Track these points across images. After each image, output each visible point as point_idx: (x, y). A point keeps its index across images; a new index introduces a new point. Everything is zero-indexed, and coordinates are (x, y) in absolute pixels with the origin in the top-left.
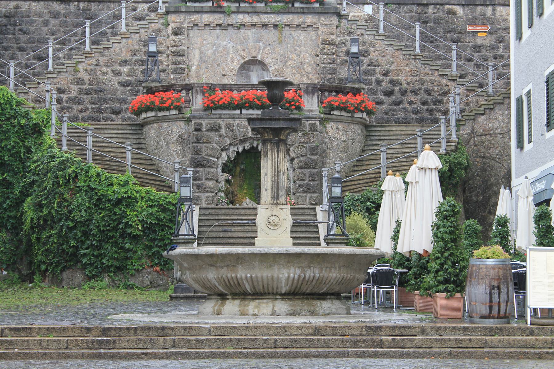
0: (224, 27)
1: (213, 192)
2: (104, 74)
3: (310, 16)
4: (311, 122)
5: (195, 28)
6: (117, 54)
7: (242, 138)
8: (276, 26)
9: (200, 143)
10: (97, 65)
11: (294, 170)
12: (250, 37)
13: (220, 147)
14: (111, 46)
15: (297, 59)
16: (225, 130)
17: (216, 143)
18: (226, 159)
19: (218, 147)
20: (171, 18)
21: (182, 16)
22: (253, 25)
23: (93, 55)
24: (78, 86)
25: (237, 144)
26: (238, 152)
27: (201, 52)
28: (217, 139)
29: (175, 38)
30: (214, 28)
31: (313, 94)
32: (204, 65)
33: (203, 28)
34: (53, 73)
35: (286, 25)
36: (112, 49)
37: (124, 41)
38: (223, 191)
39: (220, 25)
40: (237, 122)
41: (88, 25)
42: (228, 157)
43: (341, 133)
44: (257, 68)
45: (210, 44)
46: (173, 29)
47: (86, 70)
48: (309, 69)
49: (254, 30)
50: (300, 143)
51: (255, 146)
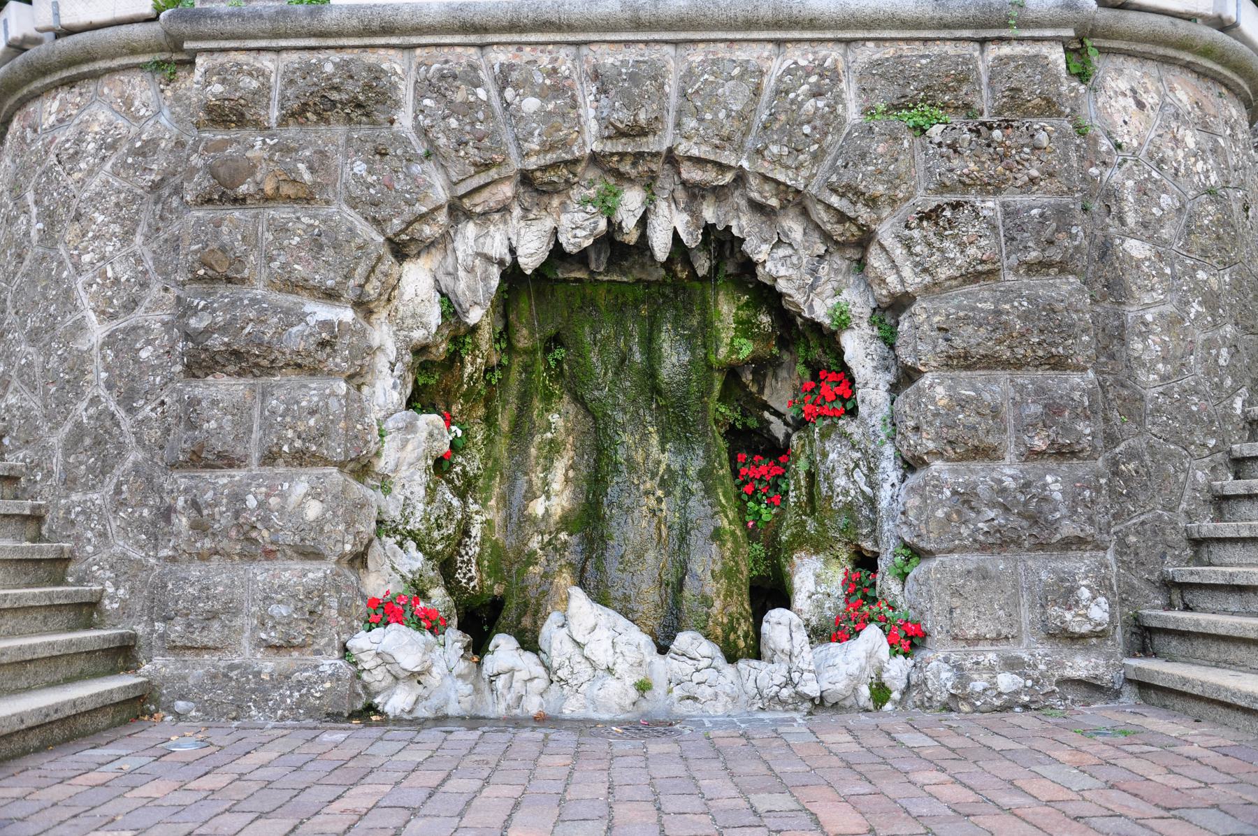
1: (310, 554)
7: (532, 163)
9: (239, 201)
11: (906, 377)
17: (353, 203)
18: (434, 316)
25: (504, 209)
26: (512, 274)
28: (360, 167)
38: (412, 535)
40: (499, 57)
43: (1190, 142)
50: (943, 188)
51: (629, 222)
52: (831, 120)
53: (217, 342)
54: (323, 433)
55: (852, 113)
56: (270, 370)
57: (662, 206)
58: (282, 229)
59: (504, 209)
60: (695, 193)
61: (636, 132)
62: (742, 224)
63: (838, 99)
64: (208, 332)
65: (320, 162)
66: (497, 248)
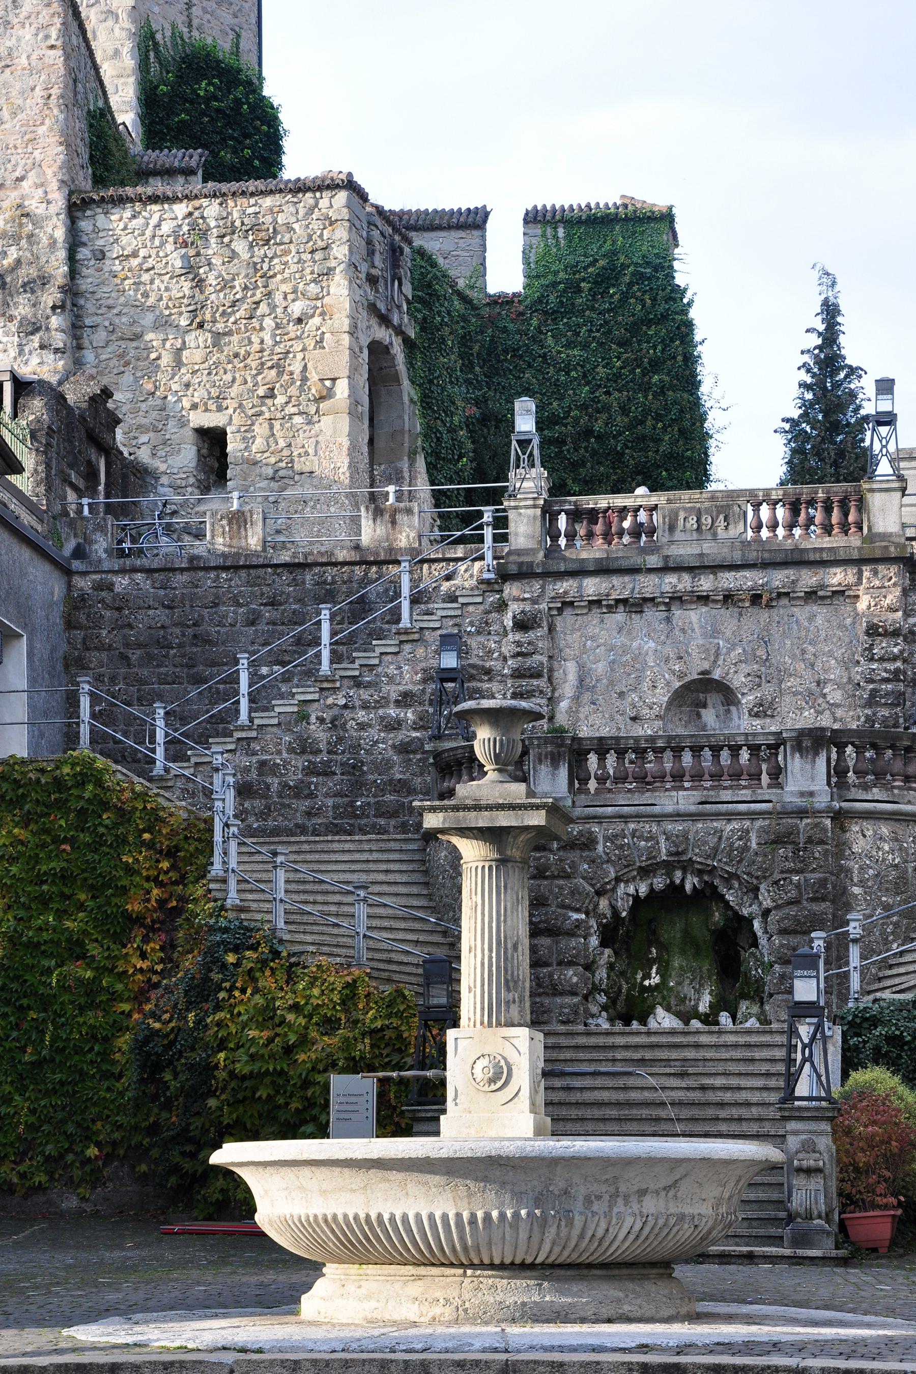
0: (633, 605)
1: (574, 994)
2: (362, 726)
3: (838, 570)
4: (809, 821)
5: (568, 612)
6: (391, 679)
7: (643, 864)
8: (756, 599)
9: (546, 878)
10: (345, 706)
12: (696, 626)
13: (593, 886)
14: (376, 661)
15: (808, 674)
16: (605, 846)
17: (583, 878)
19: (589, 888)
20: (511, 590)
21: (537, 585)
22: (704, 599)
23: (338, 685)
24: (305, 757)
25: (634, 878)
27: (581, 667)
28: (586, 866)
29: (518, 636)
30: (611, 609)
31: (816, 754)
32: (586, 697)
33: (585, 611)
34: (250, 729)
35: (780, 595)
36: (380, 669)
37: (407, 647)
38: (603, 990)
39: (625, 601)
40: (632, 826)
41: (325, 615)
42: (614, 909)
44: (713, 699)
45: (603, 648)
46: (514, 617)
47: (321, 720)
48: (836, 696)
49: (704, 609)
51: (678, 881)
52: (746, 848)
53: (542, 926)
54: (576, 956)
55: (754, 845)
56: (558, 935)
57: (689, 876)
58: (561, 888)
59: (634, 878)
60: (700, 873)
61: (677, 854)
62: (717, 882)
63: (749, 840)
64: (540, 922)
65: (573, 865)
66: (631, 890)
